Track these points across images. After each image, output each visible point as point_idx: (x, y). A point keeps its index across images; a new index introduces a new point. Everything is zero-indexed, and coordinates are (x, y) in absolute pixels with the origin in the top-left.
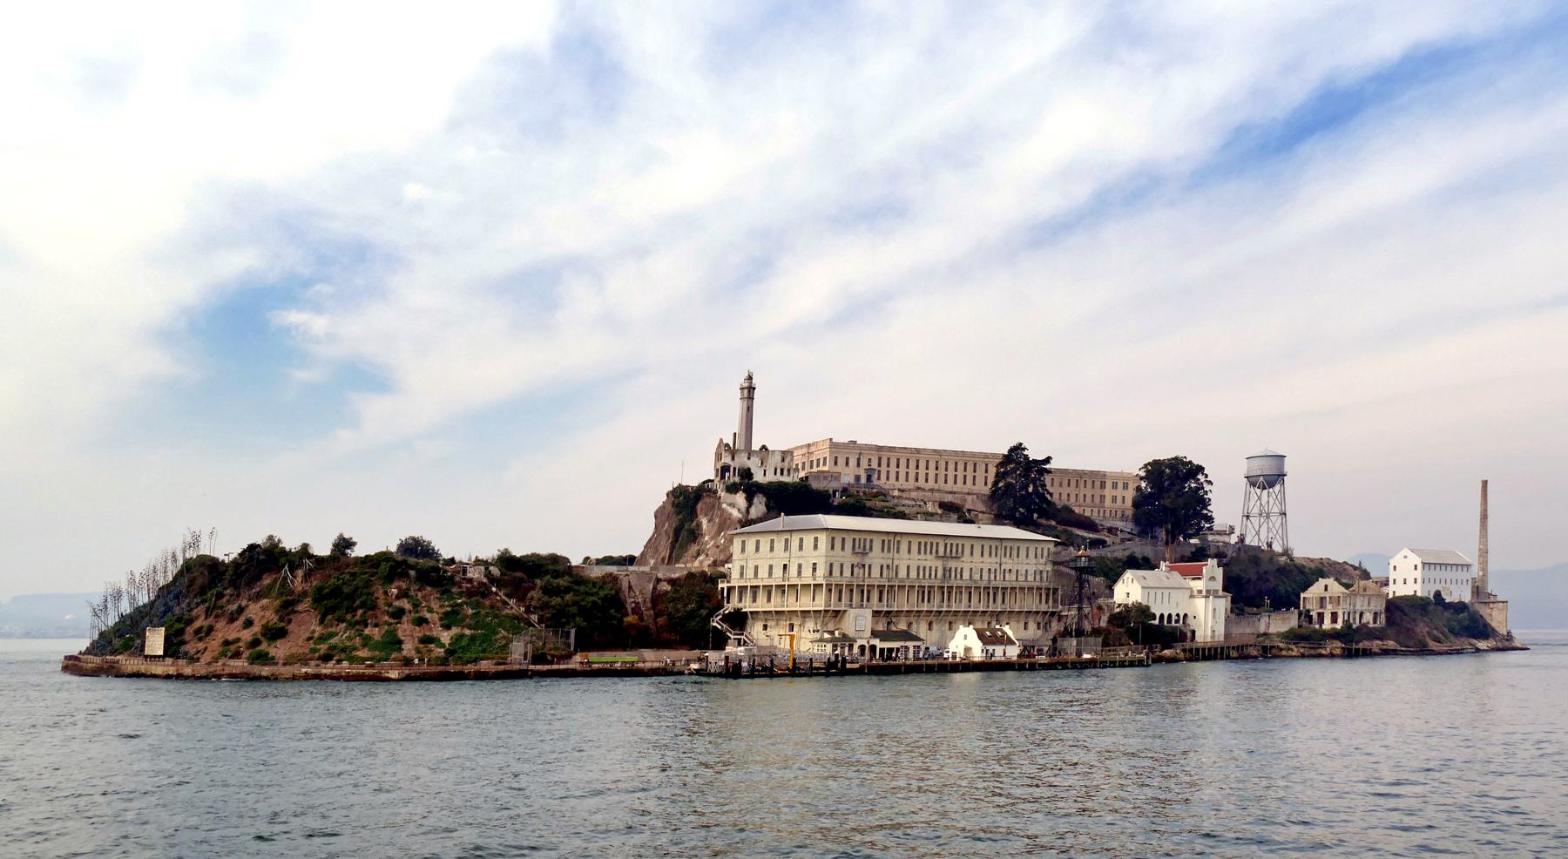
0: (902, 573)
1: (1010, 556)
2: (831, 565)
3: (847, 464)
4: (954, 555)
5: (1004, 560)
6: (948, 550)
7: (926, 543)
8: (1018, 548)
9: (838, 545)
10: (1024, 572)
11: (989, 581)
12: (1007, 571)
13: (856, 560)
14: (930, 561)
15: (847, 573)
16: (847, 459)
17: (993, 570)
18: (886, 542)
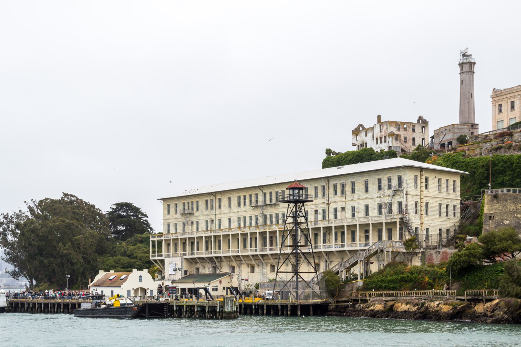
0: (225, 225)
1: (343, 192)
2: (169, 225)
3: (513, 107)
4: (274, 201)
5: (332, 199)
6: (268, 198)
7: (245, 196)
8: (353, 184)
9: (172, 210)
10: (363, 208)
11: (316, 222)
12: (339, 209)
13: (183, 219)
14: (248, 211)
15: (180, 230)
16: (513, 103)
17: (320, 211)
18: (242, 198)
